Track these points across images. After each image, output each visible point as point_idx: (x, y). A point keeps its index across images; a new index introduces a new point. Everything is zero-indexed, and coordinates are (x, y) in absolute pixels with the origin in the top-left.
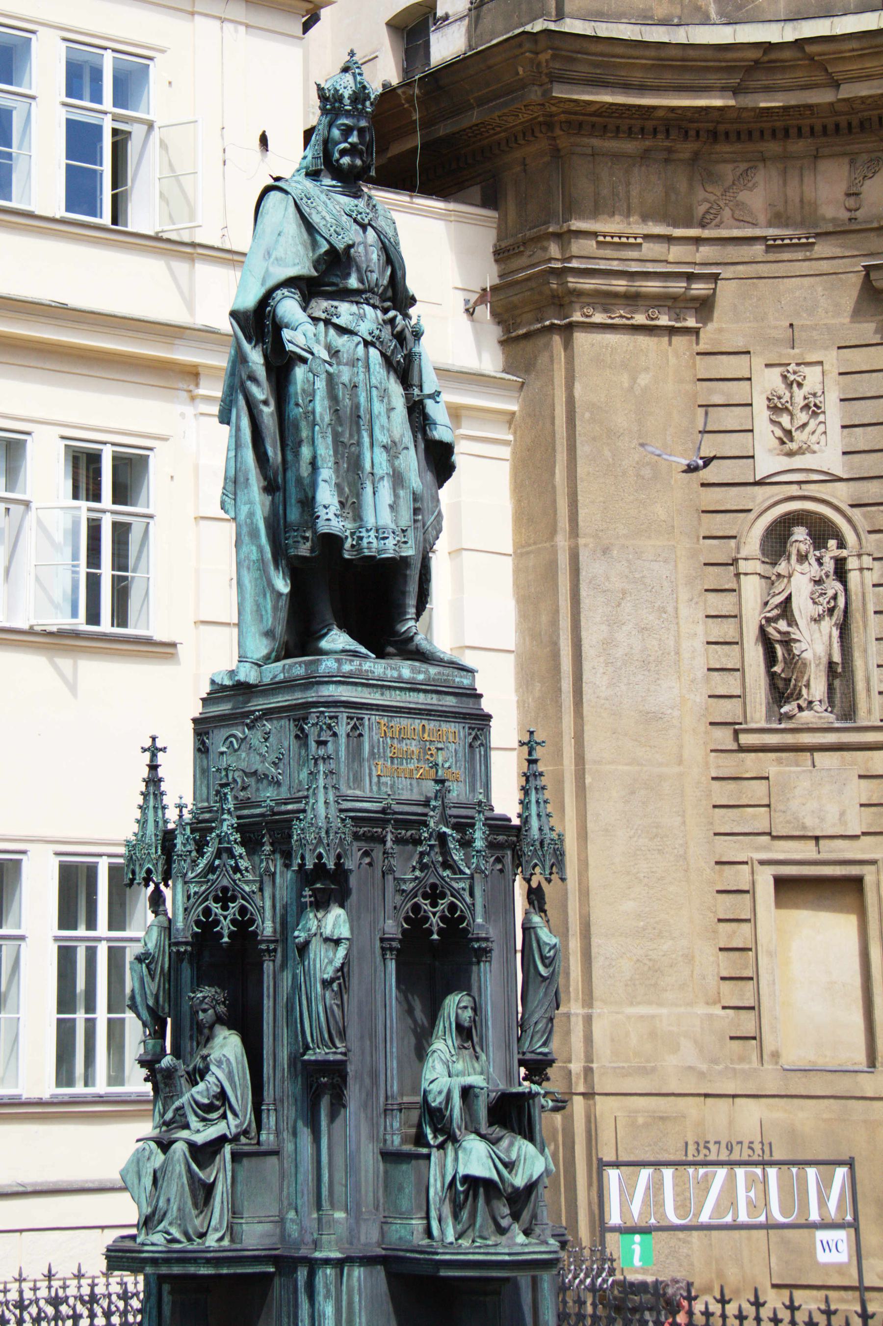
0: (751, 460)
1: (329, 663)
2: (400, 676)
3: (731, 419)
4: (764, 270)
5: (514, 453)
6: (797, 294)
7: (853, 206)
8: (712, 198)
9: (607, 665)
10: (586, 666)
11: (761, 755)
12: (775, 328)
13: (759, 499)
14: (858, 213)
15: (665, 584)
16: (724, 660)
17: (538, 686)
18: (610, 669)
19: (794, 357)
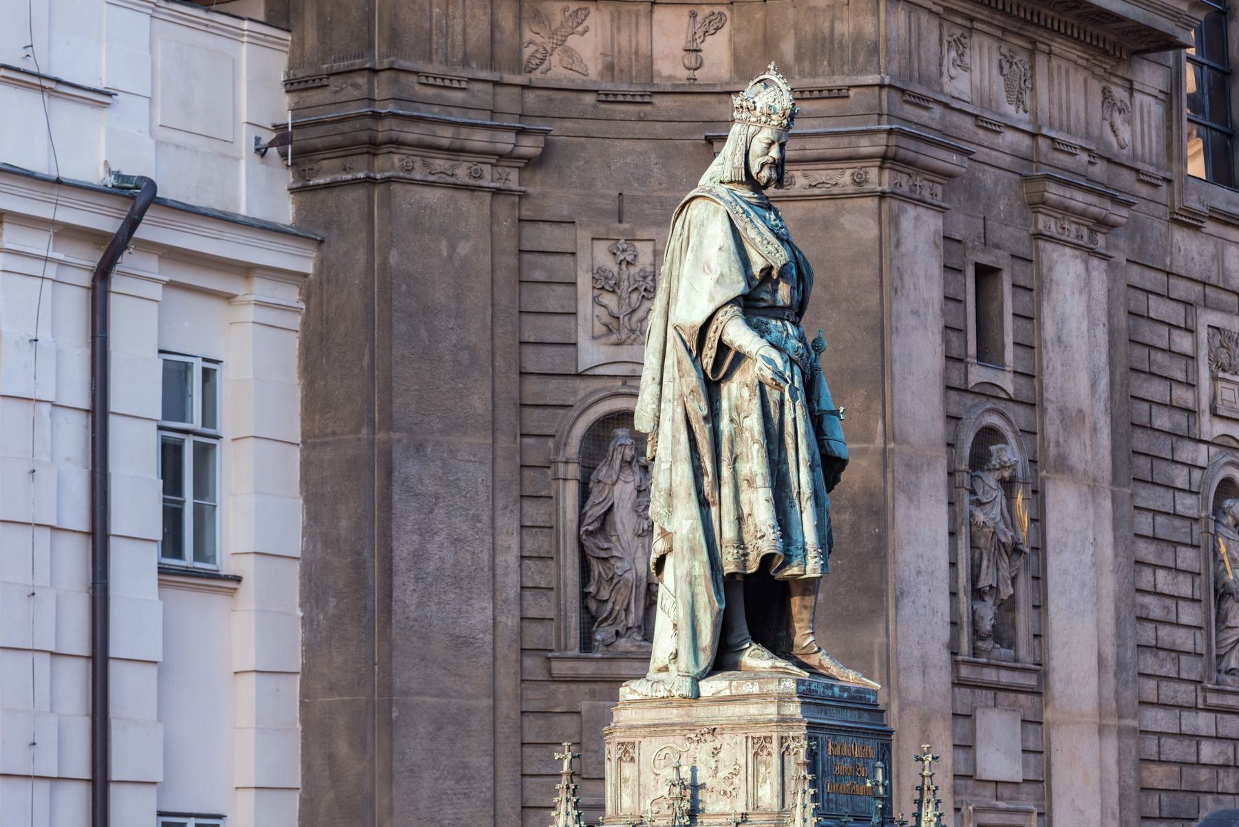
0: (571, 349)
1: (787, 684)
2: (833, 696)
3: (552, 299)
4: (592, 127)
5: (305, 323)
6: (629, 160)
7: (693, 65)
8: (538, 39)
9: (417, 579)
10: (397, 581)
11: (573, 686)
12: (603, 197)
13: (581, 394)
14: (696, 73)
15: (481, 488)
16: (537, 577)
17: (333, 602)
18: (421, 586)
19: (623, 233)
